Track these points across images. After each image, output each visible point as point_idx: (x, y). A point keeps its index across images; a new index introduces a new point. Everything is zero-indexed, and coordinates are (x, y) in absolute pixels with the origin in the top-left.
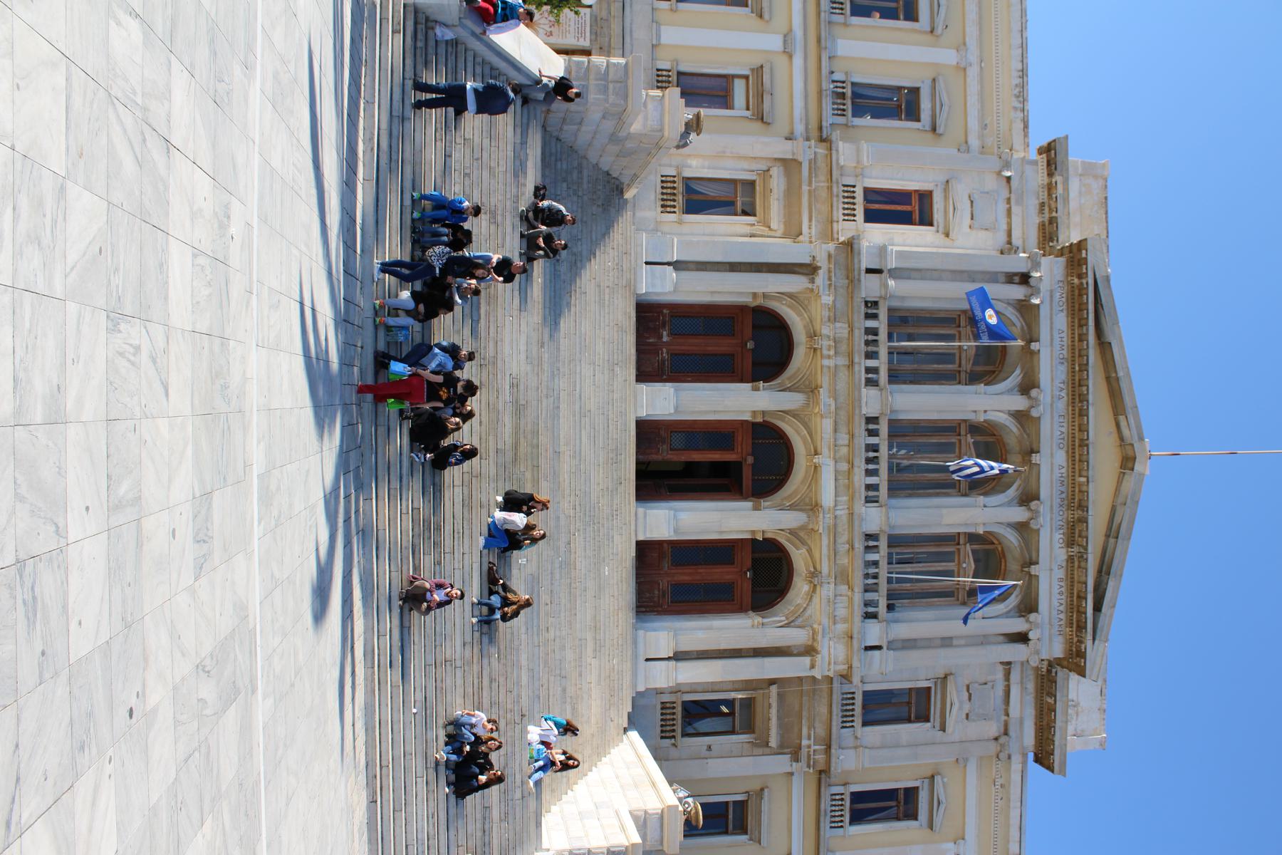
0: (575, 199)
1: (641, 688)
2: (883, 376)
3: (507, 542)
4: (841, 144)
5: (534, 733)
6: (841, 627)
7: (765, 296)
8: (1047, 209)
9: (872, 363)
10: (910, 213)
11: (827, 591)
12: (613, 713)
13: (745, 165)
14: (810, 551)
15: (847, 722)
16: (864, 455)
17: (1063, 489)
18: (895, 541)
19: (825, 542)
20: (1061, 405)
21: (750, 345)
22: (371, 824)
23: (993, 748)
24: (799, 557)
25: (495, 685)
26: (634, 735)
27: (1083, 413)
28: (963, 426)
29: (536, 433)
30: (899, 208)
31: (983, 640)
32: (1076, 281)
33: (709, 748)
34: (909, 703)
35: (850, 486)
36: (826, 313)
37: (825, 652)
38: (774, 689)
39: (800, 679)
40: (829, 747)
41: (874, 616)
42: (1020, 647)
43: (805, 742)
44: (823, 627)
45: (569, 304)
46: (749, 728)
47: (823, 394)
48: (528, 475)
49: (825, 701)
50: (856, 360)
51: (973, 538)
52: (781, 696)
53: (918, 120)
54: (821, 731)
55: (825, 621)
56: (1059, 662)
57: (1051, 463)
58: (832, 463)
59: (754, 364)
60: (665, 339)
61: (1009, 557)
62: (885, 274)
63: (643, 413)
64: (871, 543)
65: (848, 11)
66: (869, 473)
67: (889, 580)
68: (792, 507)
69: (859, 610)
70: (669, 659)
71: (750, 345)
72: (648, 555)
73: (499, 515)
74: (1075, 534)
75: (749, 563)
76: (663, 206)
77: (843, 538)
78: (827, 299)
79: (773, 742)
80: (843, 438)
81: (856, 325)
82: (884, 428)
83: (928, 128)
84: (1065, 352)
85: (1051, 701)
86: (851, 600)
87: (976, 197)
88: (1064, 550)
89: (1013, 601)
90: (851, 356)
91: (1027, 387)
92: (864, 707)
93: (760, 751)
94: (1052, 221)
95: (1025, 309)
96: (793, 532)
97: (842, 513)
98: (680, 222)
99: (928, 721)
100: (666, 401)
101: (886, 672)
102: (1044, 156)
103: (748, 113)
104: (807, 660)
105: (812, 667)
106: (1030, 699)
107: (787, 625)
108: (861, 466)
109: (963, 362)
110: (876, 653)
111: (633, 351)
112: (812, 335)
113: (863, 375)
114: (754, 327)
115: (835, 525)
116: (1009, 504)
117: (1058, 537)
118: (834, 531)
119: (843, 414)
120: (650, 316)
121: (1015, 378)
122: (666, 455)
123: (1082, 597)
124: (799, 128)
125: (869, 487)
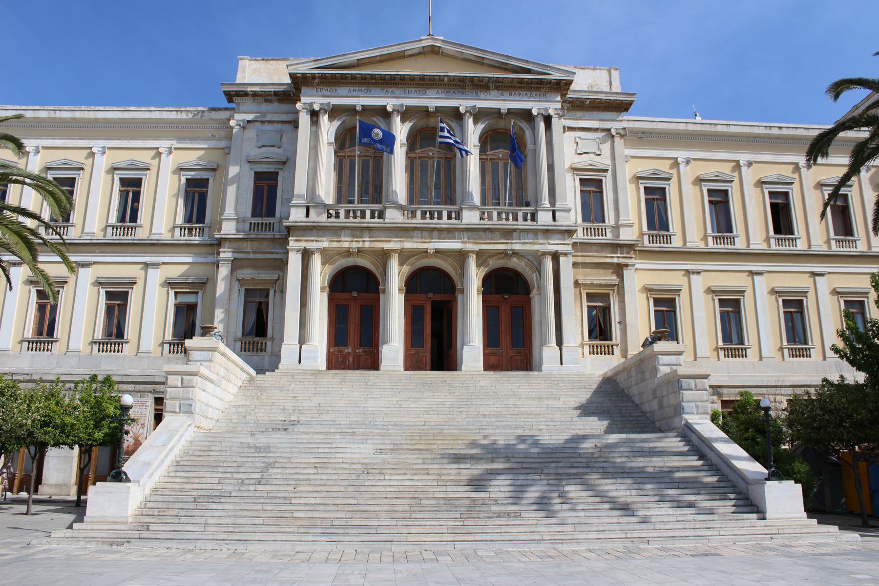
0: (257, 410)
4: (222, 232)
8: (269, 98)
10: (268, 185)
13: (235, 296)
14: (490, 257)
17: (452, 92)
25: (575, 465)
27: (403, 78)
28: (410, 155)
30: (265, 194)
32: (317, 80)
47: (387, 246)
53: (208, 180)
57: (434, 101)
59: (367, 292)
60: (350, 350)
61: (495, 127)
65: (134, 224)
67: (510, 205)
70: (561, 349)
71: (355, 294)
74: (480, 86)
76: (261, 351)
83: (213, 173)
84: (363, 89)
87: (260, 144)
88: (492, 92)
89: (524, 125)
94: (276, 93)
95: (334, 112)
98: (273, 339)
102: (234, 98)
103: (200, 293)
104: (562, 259)
105: (565, 254)
106: (587, 114)
109: (368, 154)
110: (557, 214)
111: (358, 372)
113: (376, 220)
117: (482, 96)
120: (335, 363)
122: (426, 352)
124: (210, 259)
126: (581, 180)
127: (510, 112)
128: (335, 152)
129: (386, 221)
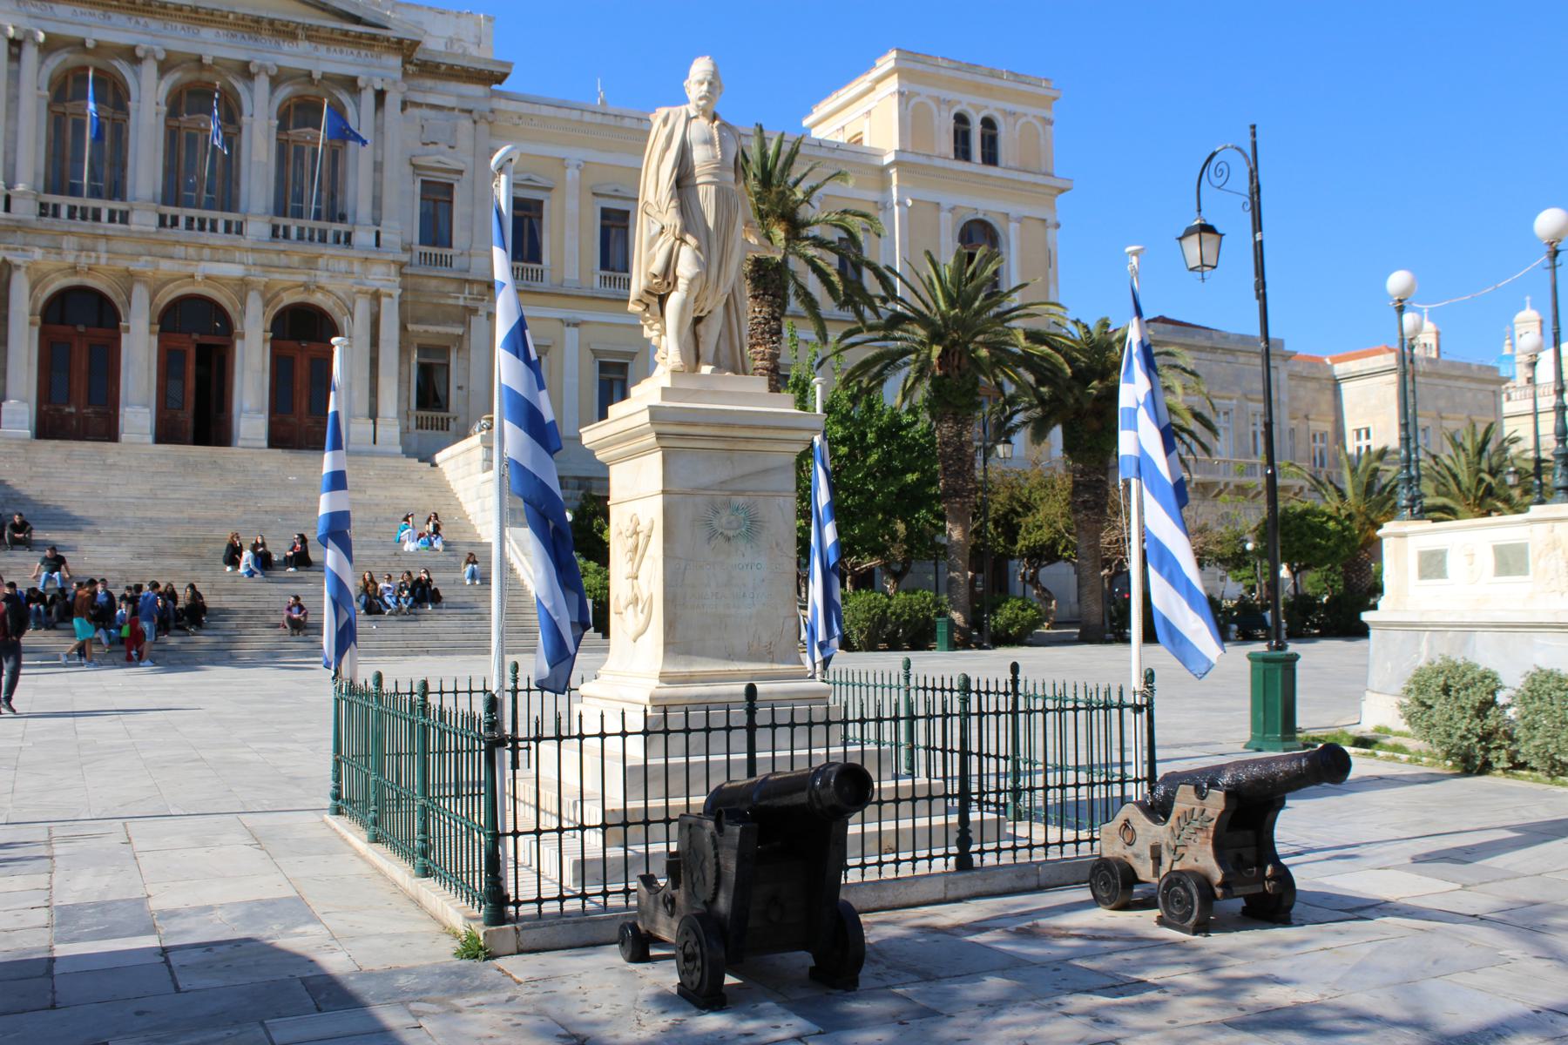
1: (399, 449)
2: (117, 205)
3: (264, 561)
5: (410, 546)
6: (357, 267)
7: (32, 314)
9: (105, 216)
11: (323, 278)
12: (415, 476)
14: (285, 289)
15: (446, 262)
16: (196, 232)
18: (280, 209)
19: (277, 276)
20: (154, 25)
21: (81, 328)
22: (443, 653)
23: (483, 126)
24: (288, 299)
26: (439, 457)
29: (177, 540)
31: (379, 130)
33: (460, 388)
34: (435, 201)
35: (226, 249)
36: (53, 257)
37: (378, 284)
38: (410, 327)
39: (400, 304)
40: (467, 281)
41: (348, 236)
42: (388, 98)
43: (461, 302)
44: (356, 280)
45: (57, 508)
46: (444, 351)
47: (135, 266)
48: (211, 546)
49: (425, 281)
50: (101, 232)
51: (282, 127)
52: (418, 321)
54: (451, 287)
55: (351, 281)
56: (407, 60)
57: (214, 45)
58: (203, 264)
60: (73, 410)
62: (11, 192)
63: (150, 438)
64: (281, 232)
66: (214, 229)
67: (318, 217)
68: (243, 303)
69: (340, 250)
71: (81, 328)
72: (280, 438)
73: (242, 570)
75: (293, 344)
77: (274, 259)
78: (38, 254)
79: (459, 331)
80: (179, 251)
81: (66, 228)
82: (170, 211)
85: (443, 68)
86: (332, 256)
89: (345, 98)
90: (96, 236)
91: (131, 56)
92: (435, 244)
93: (465, 342)
95: (50, 46)
96: (266, 304)
97: (250, 258)
99: (451, 185)
100: (137, 417)
101: (402, 223)
104: (384, 300)
105: (390, 296)
106: (441, 85)
107: (352, 315)
108: (206, 237)
110: (382, 236)
111: (89, 444)
112: (74, 270)
114: (62, 323)
115: (262, 265)
116: (251, 90)
117: (286, 46)
118: (268, 267)
119: (156, 249)
120: (49, 426)
121: (123, 67)
122: (187, 416)
123: (346, 33)
125: (228, 230)
126: (423, 182)
127: (325, 77)
128: (49, 106)
129: (133, 227)
